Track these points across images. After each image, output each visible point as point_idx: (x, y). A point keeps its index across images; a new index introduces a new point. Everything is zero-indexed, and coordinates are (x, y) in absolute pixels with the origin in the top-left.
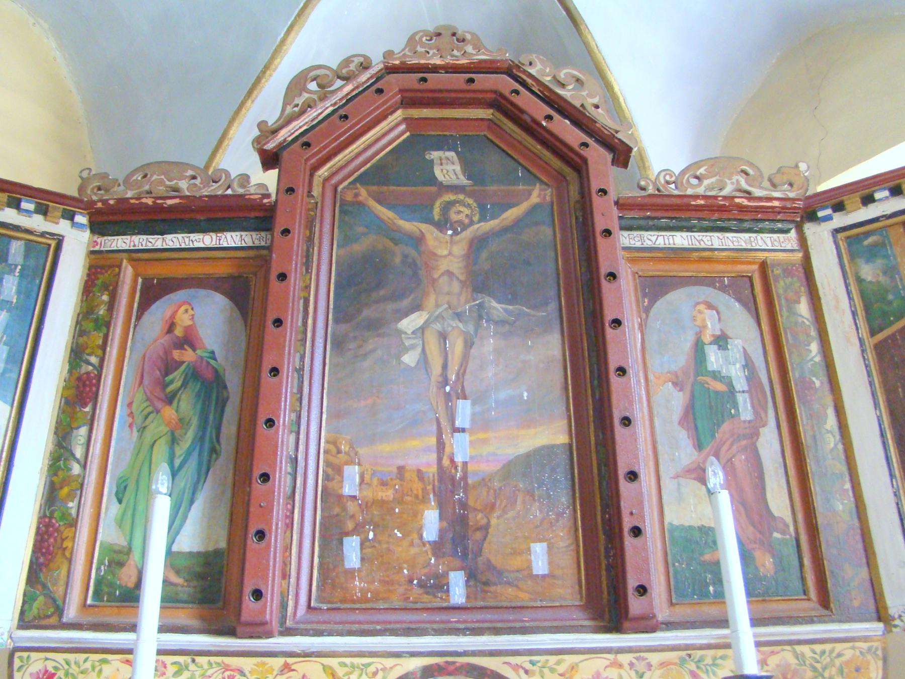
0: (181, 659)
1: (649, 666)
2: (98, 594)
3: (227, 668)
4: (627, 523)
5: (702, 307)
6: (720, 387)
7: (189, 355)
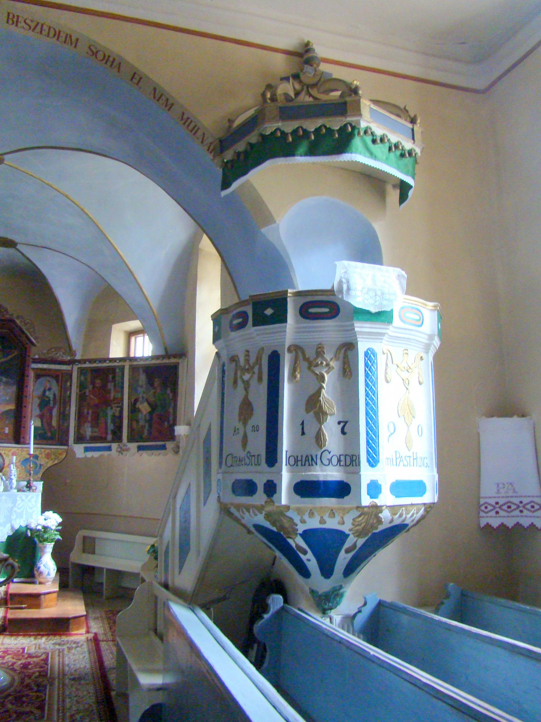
1: (24, 451)
4: (23, 426)
5: (47, 382)
6: (47, 399)
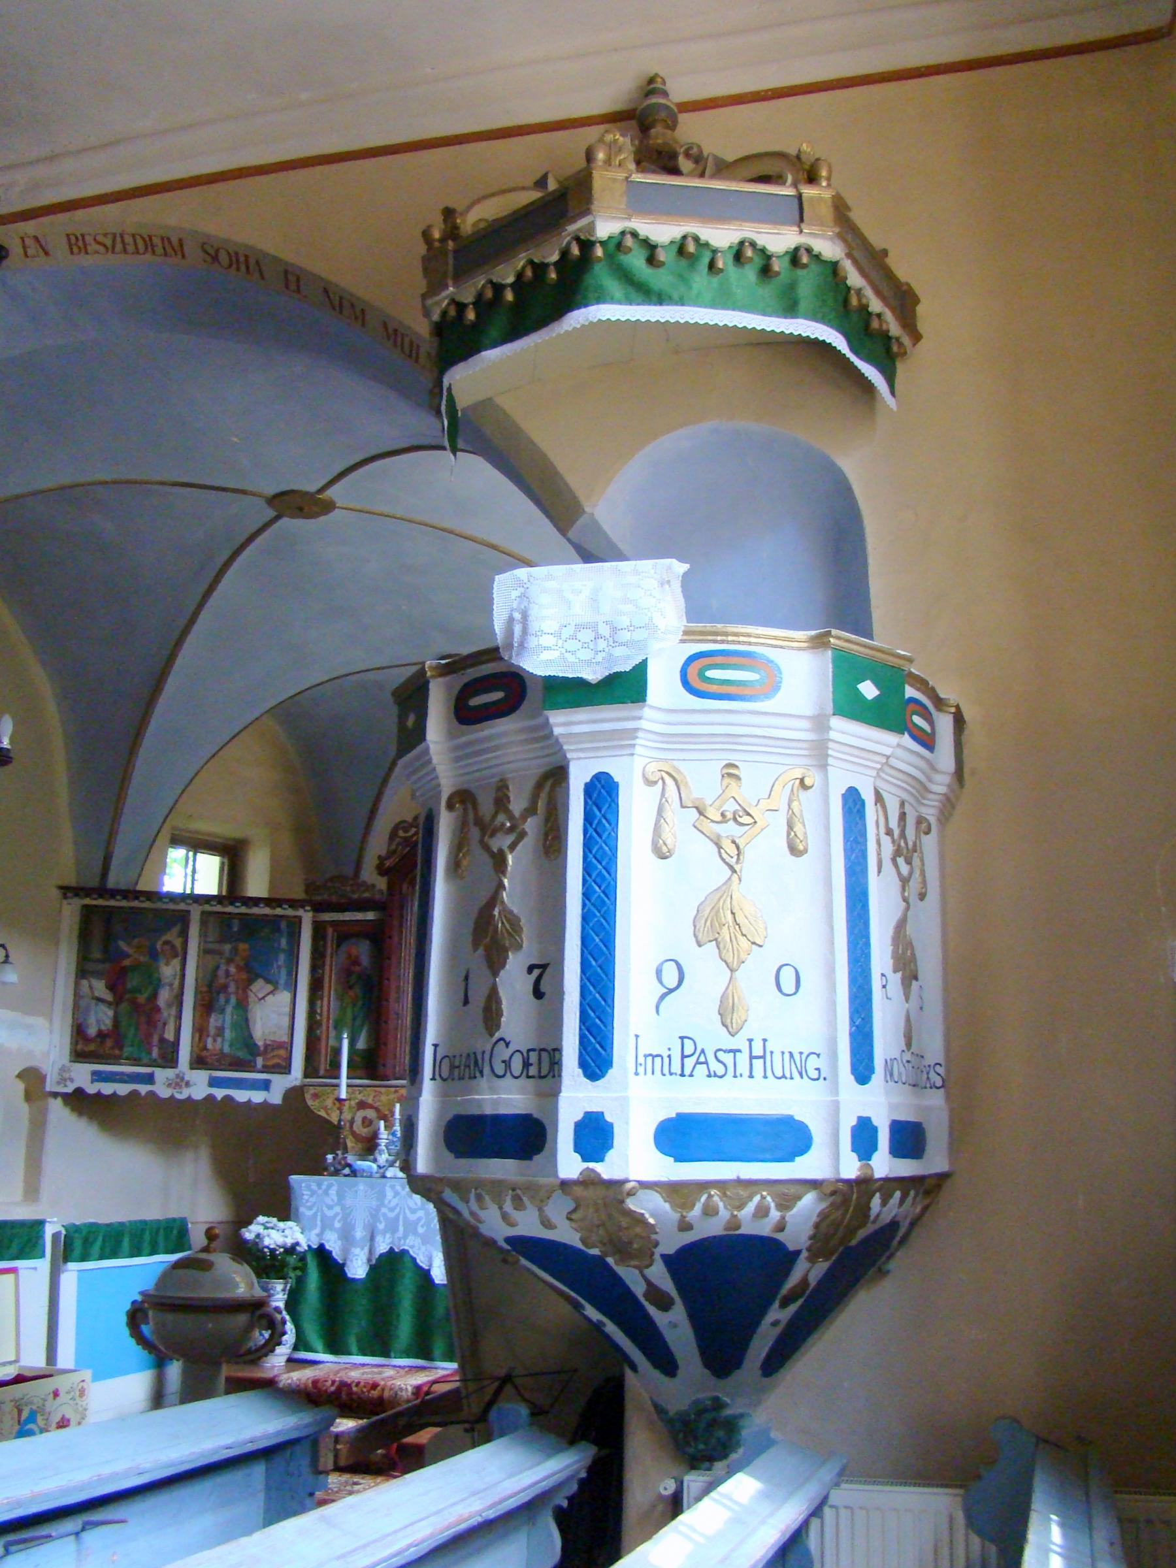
0: (360, 1088)
2: (330, 1065)
3: (376, 1091)
7: (357, 969)
